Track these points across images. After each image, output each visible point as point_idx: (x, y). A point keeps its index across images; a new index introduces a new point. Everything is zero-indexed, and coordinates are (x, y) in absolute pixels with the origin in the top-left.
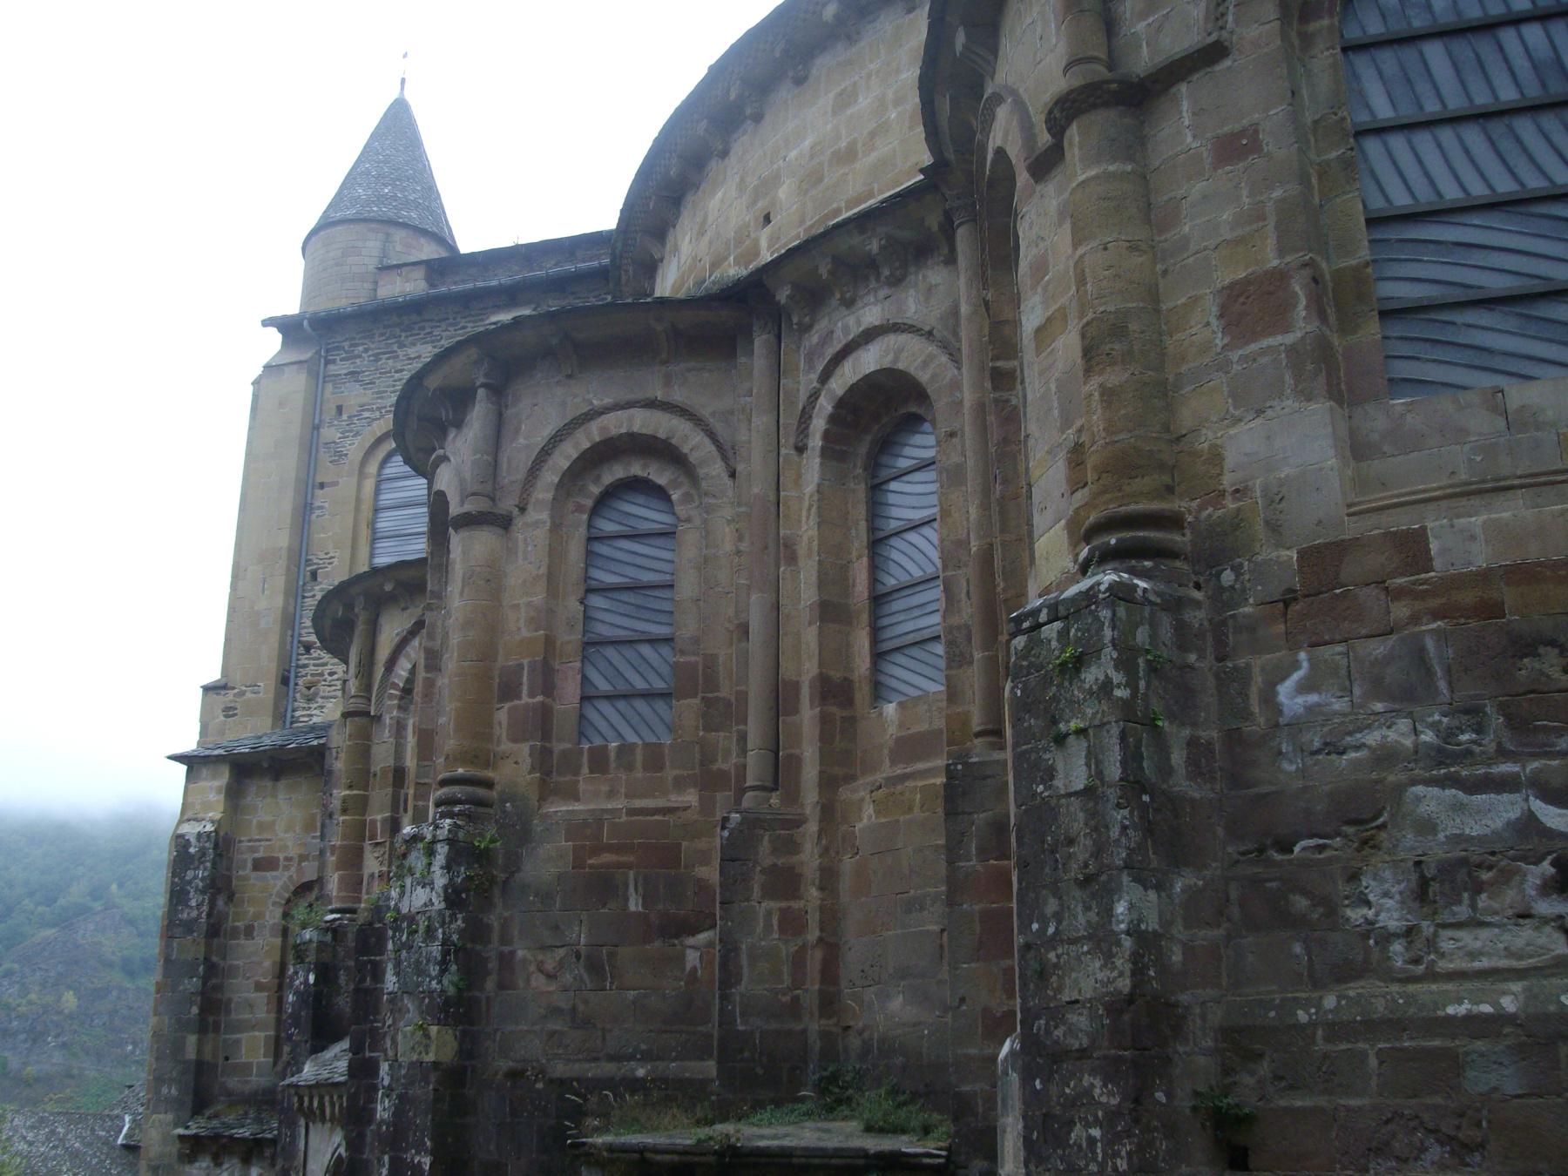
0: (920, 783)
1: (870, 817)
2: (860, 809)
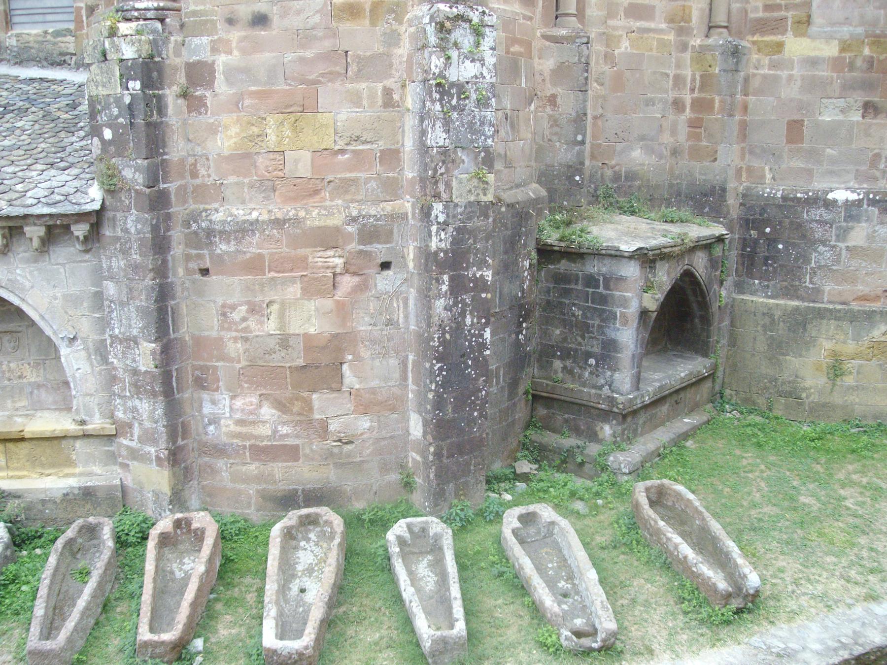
0: (657, 36)
1: (626, 48)
2: (619, 41)
